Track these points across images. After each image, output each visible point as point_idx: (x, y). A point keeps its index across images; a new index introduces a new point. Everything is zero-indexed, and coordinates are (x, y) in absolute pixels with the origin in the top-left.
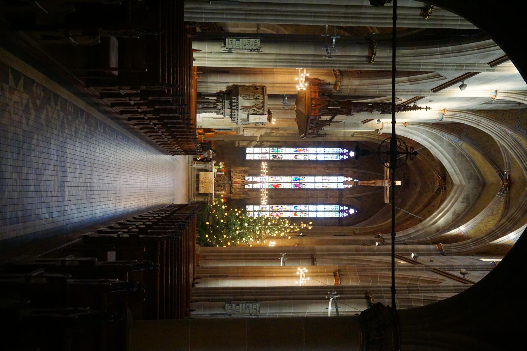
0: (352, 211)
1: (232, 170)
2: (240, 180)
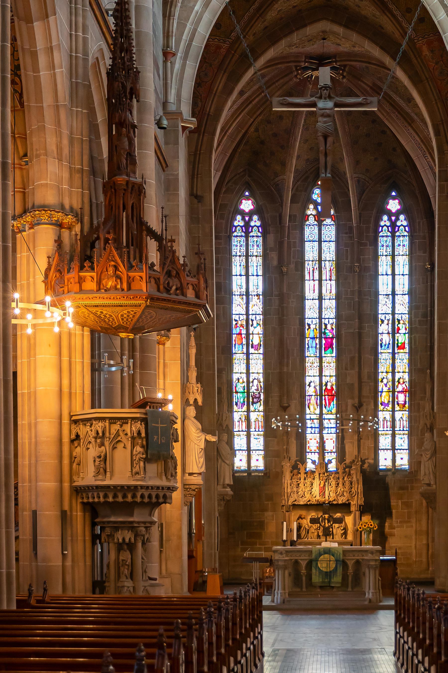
0: (394, 205)
1: (290, 503)
2: (316, 482)
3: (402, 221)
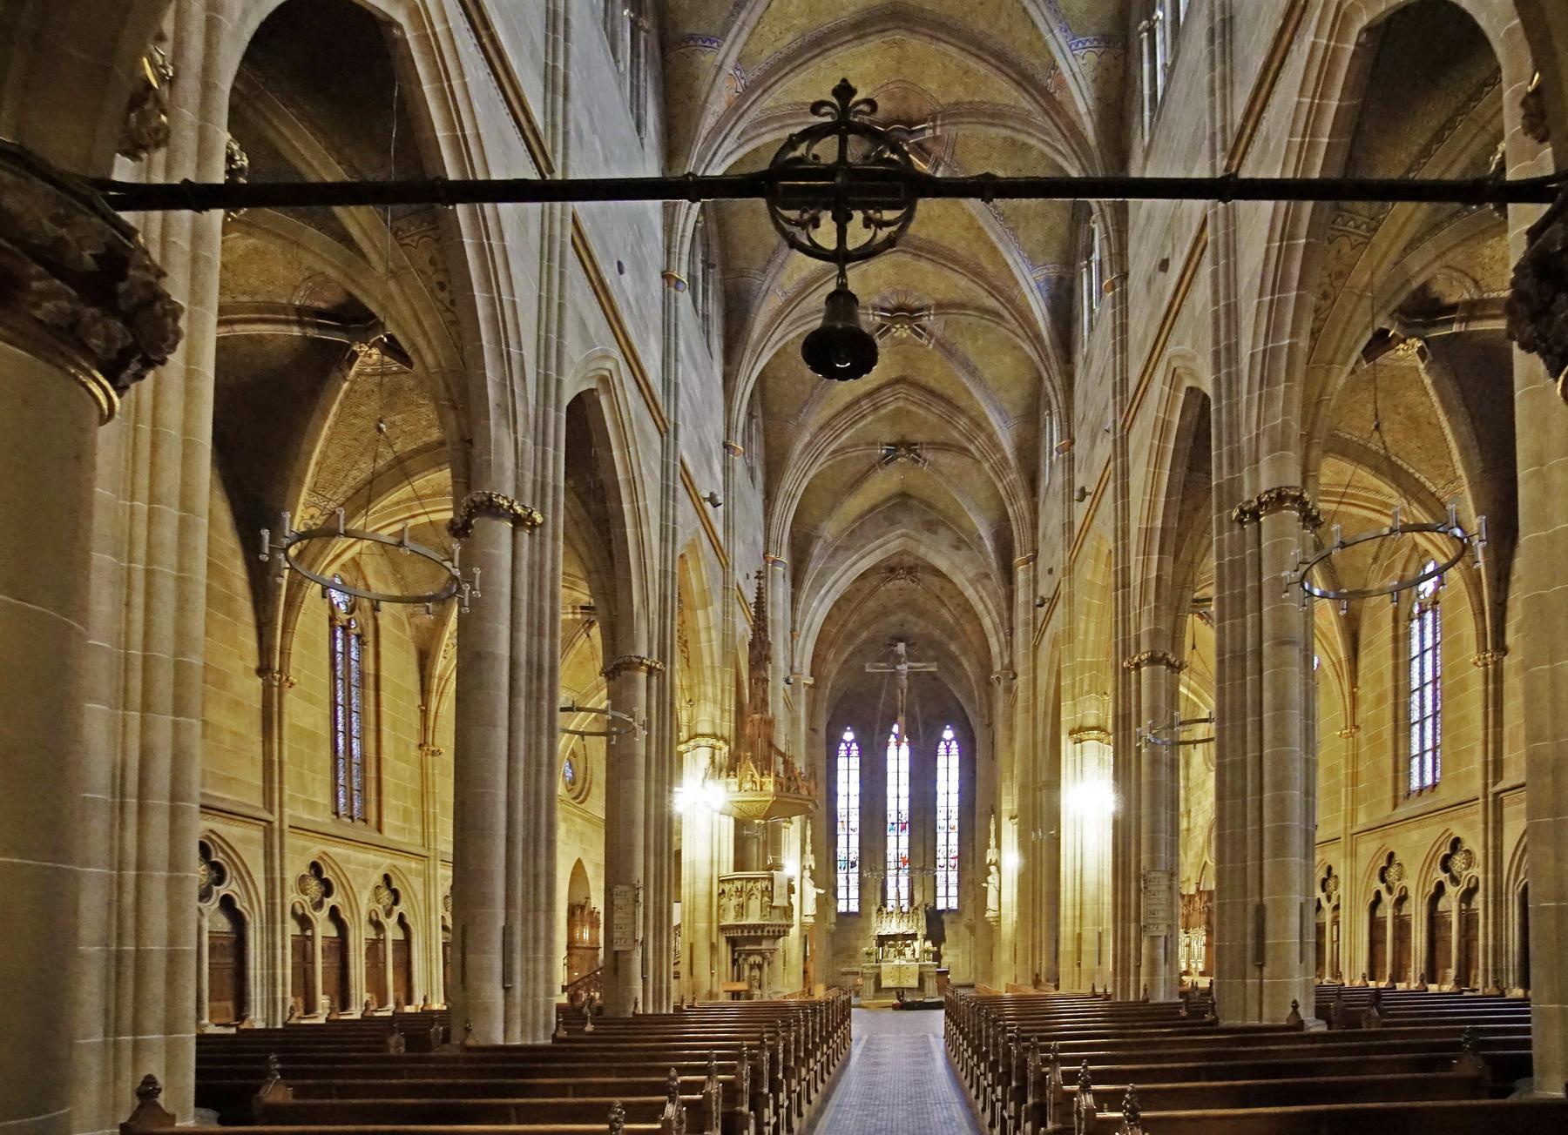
3: (954, 745)
